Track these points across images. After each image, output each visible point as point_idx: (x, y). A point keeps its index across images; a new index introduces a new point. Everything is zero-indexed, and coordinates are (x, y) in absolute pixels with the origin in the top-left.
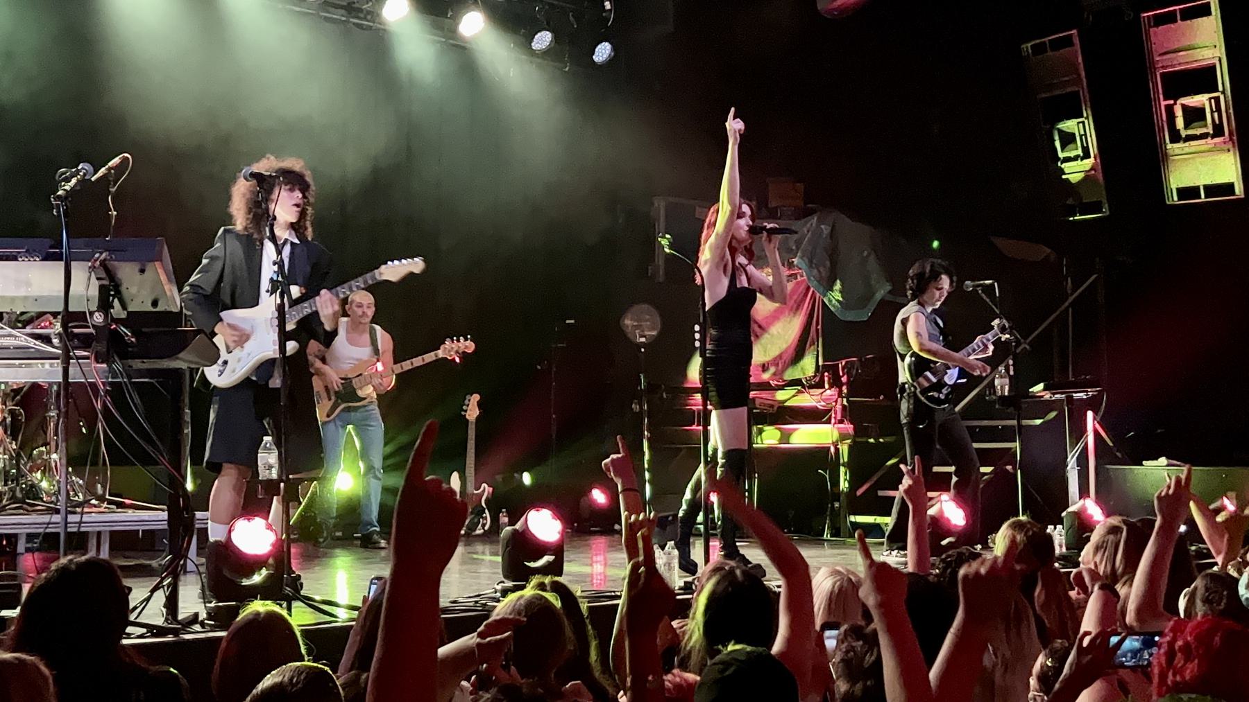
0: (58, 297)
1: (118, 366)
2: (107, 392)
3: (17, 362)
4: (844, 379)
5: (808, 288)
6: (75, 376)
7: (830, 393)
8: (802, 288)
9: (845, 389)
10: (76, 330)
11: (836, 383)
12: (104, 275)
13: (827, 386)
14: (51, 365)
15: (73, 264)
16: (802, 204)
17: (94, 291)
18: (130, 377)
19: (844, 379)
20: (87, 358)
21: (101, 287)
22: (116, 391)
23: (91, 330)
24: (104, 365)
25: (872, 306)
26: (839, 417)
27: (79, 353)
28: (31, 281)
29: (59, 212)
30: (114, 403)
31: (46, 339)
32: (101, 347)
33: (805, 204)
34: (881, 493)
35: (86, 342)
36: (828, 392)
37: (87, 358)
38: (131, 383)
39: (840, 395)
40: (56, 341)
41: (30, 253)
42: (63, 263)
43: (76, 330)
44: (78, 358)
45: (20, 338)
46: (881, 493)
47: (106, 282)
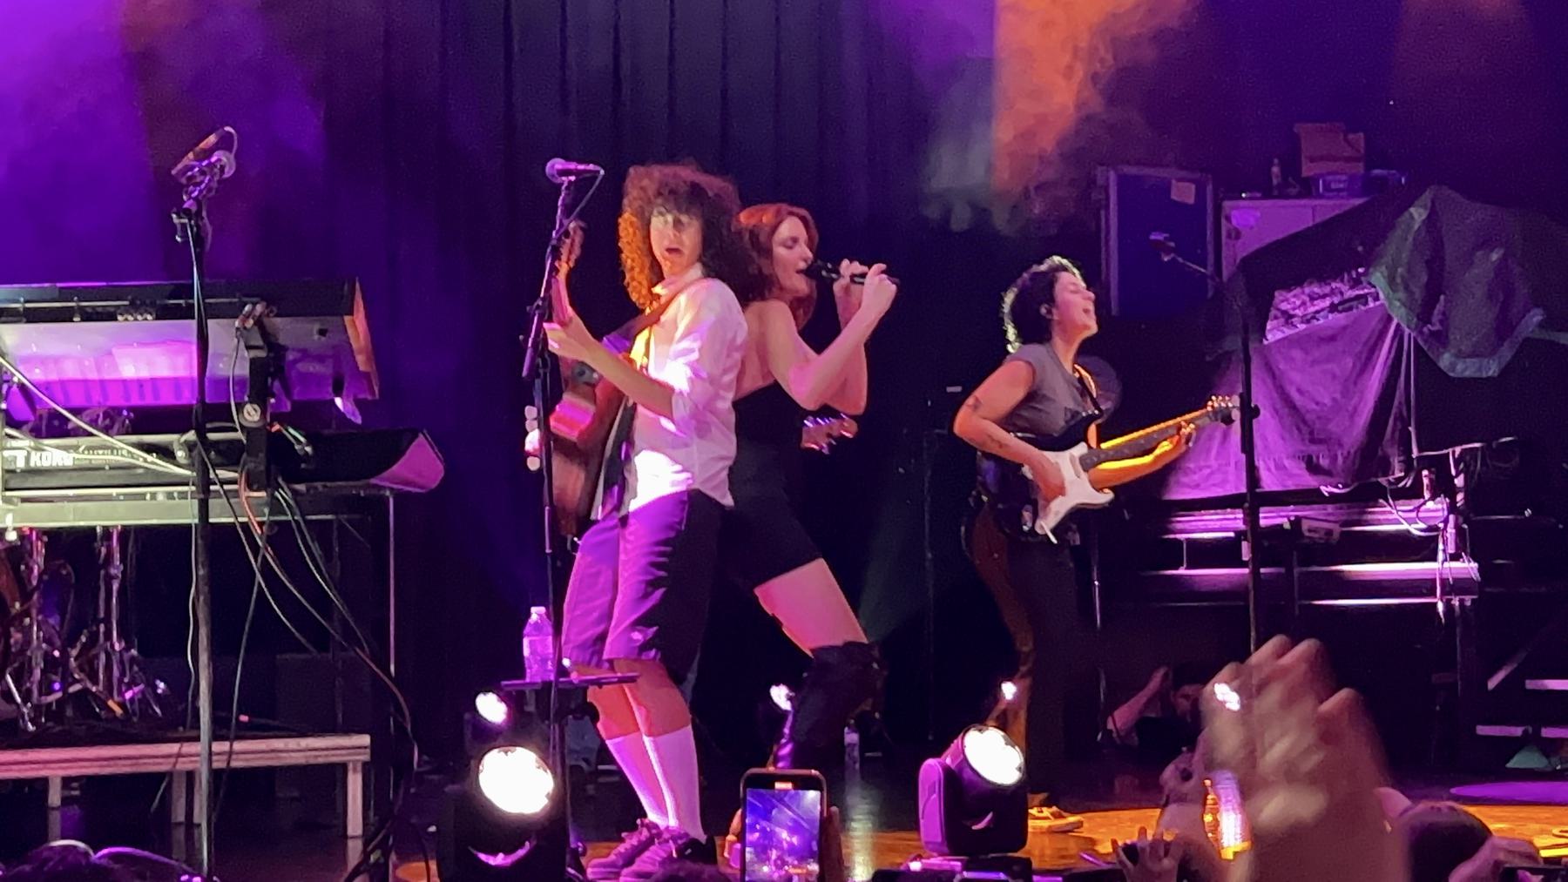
0: (192, 379)
1: (284, 495)
2: (270, 540)
3: (114, 491)
4: (1459, 482)
5: (1390, 319)
6: (220, 515)
7: (1435, 507)
8: (1375, 323)
9: (1460, 497)
10: (212, 436)
11: (1442, 487)
12: (260, 343)
13: (1427, 495)
14: (170, 496)
15: (210, 322)
16: (1360, 168)
17: (244, 370)
18: (303, 516)
19: (1459, 482)
20: (233, 482)
21: (253, 361)
22: (280, 536)
23: (239, 435)
24: (263, 494)
25: (1506, 353)
26: (1451, 550)
27: (224, 474)
28: (140, 354)
29: (185, 236)
30: (278, 556)
31: (166, 453)
32: (257, 463)
33: (1368, 168)
34: (1530, 684)
35: (230, 454)
36: (1430, 505)
37: (233, 482)
38: (307, 522)
39: (1452, 508)
40: (180, 454)
41: (135, 308)
42: (194, 323)
43: (212, 436)
44: (223, 482)
45: (122, 450)
46: (1530, 684)
47: (262, 354)
